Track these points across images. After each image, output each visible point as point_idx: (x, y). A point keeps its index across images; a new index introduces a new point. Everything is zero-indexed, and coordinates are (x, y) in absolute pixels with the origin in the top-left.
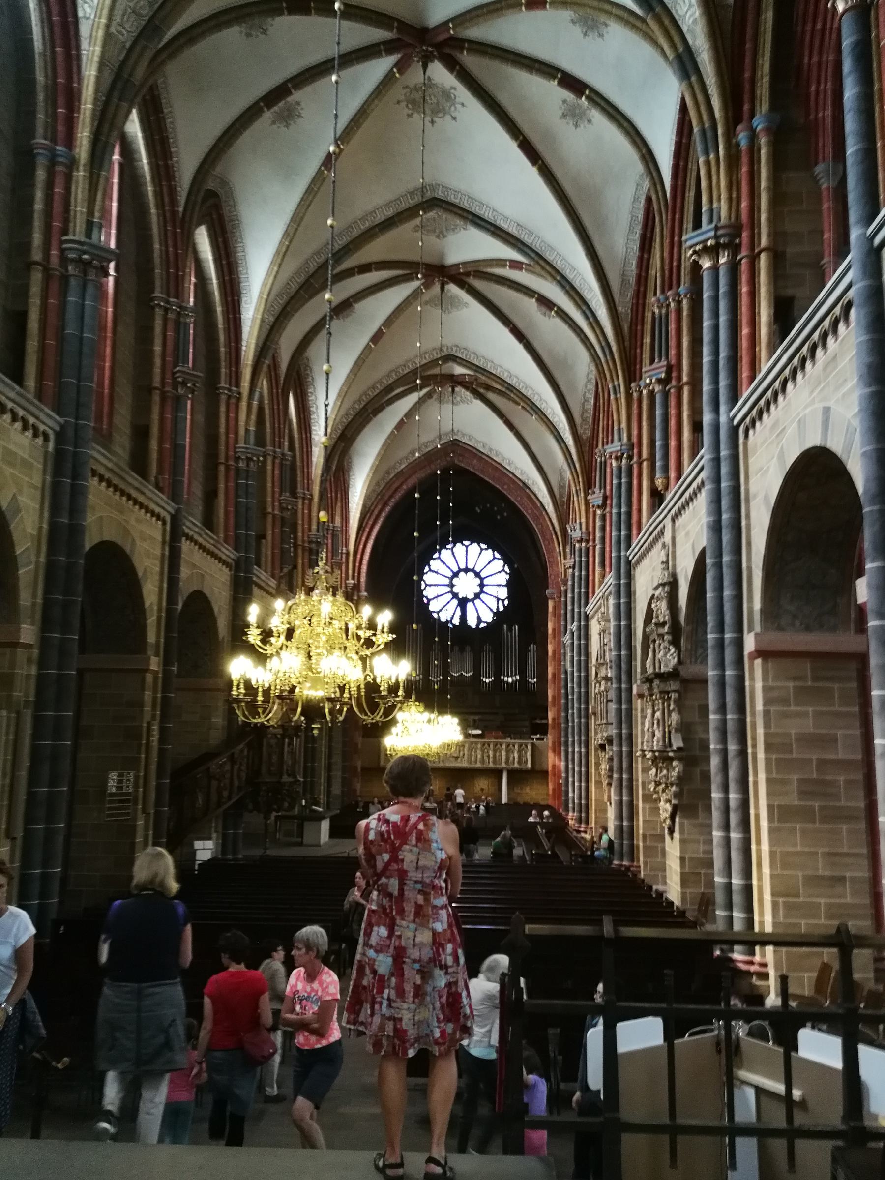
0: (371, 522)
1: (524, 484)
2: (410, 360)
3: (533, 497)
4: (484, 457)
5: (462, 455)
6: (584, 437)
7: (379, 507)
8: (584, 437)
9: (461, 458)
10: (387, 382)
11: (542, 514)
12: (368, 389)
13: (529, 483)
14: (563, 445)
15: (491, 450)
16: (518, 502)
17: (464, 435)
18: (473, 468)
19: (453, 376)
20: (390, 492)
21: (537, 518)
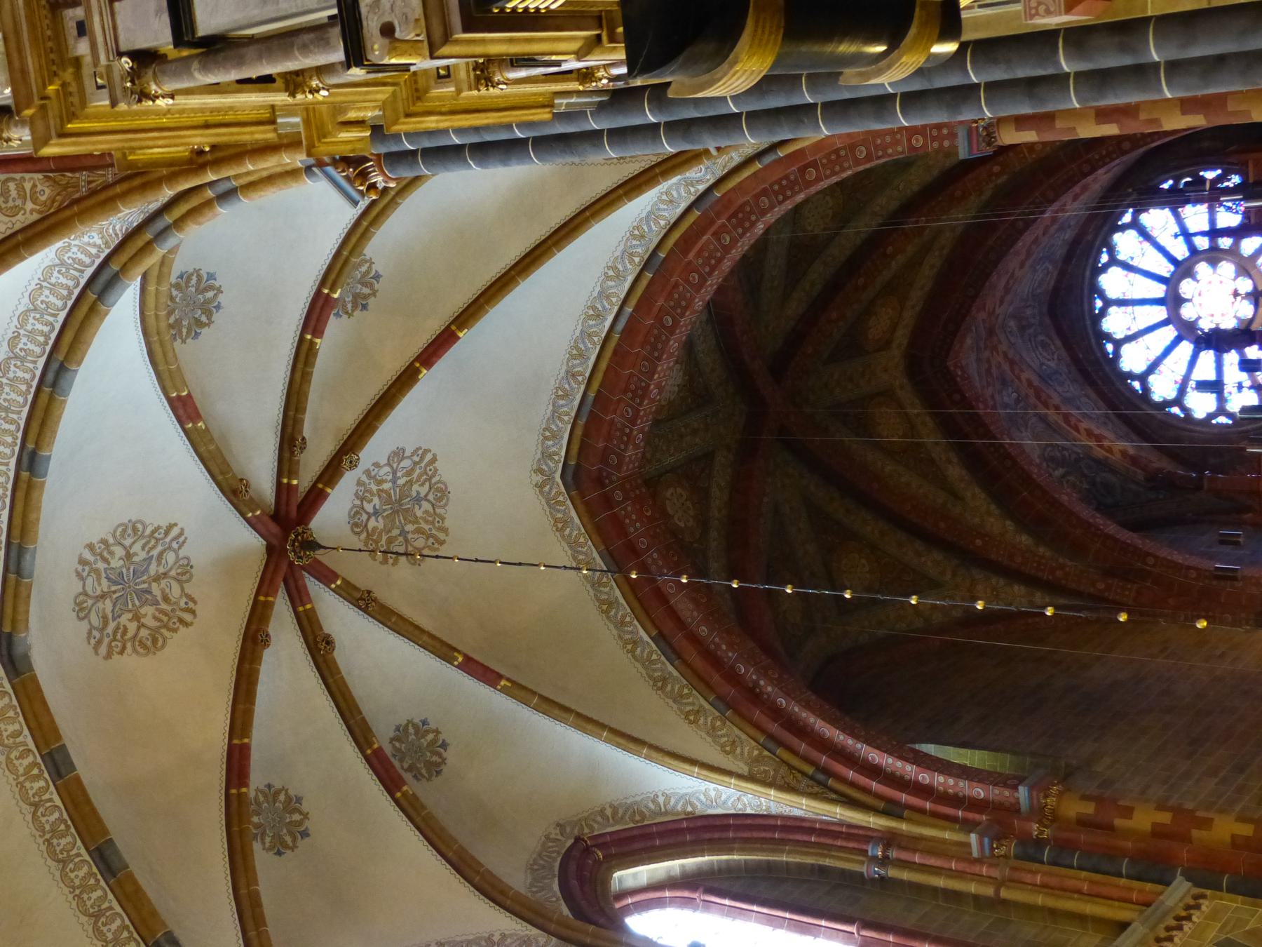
0: (803, 747)
1: (646, 266)
2: (21, 786)
3: (676, 235)
4: (592, 395)
5: (604, 459)
6: (46, 192)
7: (757, 715)
8: (46, 192)
9: (614, 460)
10: (85, 867)
11: (727, 199)
12: (98, 933)
13: (641, 251)
14: (115, 267)
15: (571, 375)
16: (703, 280)
17: (547, 455)
18: (633, 421)
19: (270, 549)
20: (716, 678)
21: (741, 216)
